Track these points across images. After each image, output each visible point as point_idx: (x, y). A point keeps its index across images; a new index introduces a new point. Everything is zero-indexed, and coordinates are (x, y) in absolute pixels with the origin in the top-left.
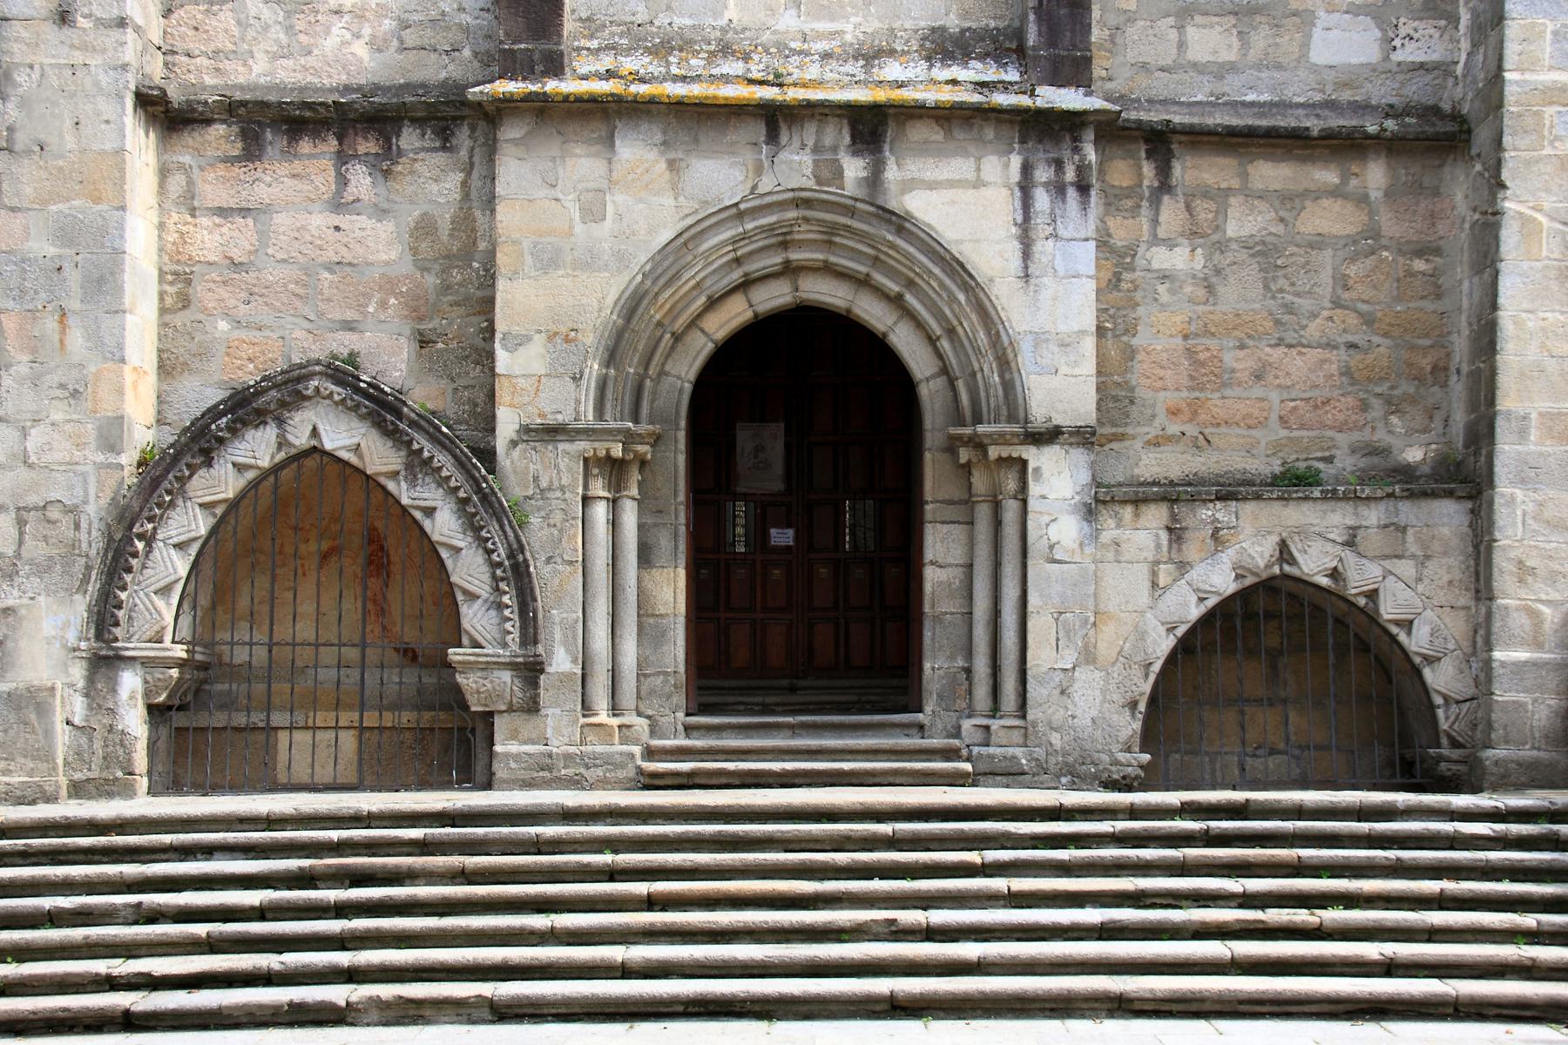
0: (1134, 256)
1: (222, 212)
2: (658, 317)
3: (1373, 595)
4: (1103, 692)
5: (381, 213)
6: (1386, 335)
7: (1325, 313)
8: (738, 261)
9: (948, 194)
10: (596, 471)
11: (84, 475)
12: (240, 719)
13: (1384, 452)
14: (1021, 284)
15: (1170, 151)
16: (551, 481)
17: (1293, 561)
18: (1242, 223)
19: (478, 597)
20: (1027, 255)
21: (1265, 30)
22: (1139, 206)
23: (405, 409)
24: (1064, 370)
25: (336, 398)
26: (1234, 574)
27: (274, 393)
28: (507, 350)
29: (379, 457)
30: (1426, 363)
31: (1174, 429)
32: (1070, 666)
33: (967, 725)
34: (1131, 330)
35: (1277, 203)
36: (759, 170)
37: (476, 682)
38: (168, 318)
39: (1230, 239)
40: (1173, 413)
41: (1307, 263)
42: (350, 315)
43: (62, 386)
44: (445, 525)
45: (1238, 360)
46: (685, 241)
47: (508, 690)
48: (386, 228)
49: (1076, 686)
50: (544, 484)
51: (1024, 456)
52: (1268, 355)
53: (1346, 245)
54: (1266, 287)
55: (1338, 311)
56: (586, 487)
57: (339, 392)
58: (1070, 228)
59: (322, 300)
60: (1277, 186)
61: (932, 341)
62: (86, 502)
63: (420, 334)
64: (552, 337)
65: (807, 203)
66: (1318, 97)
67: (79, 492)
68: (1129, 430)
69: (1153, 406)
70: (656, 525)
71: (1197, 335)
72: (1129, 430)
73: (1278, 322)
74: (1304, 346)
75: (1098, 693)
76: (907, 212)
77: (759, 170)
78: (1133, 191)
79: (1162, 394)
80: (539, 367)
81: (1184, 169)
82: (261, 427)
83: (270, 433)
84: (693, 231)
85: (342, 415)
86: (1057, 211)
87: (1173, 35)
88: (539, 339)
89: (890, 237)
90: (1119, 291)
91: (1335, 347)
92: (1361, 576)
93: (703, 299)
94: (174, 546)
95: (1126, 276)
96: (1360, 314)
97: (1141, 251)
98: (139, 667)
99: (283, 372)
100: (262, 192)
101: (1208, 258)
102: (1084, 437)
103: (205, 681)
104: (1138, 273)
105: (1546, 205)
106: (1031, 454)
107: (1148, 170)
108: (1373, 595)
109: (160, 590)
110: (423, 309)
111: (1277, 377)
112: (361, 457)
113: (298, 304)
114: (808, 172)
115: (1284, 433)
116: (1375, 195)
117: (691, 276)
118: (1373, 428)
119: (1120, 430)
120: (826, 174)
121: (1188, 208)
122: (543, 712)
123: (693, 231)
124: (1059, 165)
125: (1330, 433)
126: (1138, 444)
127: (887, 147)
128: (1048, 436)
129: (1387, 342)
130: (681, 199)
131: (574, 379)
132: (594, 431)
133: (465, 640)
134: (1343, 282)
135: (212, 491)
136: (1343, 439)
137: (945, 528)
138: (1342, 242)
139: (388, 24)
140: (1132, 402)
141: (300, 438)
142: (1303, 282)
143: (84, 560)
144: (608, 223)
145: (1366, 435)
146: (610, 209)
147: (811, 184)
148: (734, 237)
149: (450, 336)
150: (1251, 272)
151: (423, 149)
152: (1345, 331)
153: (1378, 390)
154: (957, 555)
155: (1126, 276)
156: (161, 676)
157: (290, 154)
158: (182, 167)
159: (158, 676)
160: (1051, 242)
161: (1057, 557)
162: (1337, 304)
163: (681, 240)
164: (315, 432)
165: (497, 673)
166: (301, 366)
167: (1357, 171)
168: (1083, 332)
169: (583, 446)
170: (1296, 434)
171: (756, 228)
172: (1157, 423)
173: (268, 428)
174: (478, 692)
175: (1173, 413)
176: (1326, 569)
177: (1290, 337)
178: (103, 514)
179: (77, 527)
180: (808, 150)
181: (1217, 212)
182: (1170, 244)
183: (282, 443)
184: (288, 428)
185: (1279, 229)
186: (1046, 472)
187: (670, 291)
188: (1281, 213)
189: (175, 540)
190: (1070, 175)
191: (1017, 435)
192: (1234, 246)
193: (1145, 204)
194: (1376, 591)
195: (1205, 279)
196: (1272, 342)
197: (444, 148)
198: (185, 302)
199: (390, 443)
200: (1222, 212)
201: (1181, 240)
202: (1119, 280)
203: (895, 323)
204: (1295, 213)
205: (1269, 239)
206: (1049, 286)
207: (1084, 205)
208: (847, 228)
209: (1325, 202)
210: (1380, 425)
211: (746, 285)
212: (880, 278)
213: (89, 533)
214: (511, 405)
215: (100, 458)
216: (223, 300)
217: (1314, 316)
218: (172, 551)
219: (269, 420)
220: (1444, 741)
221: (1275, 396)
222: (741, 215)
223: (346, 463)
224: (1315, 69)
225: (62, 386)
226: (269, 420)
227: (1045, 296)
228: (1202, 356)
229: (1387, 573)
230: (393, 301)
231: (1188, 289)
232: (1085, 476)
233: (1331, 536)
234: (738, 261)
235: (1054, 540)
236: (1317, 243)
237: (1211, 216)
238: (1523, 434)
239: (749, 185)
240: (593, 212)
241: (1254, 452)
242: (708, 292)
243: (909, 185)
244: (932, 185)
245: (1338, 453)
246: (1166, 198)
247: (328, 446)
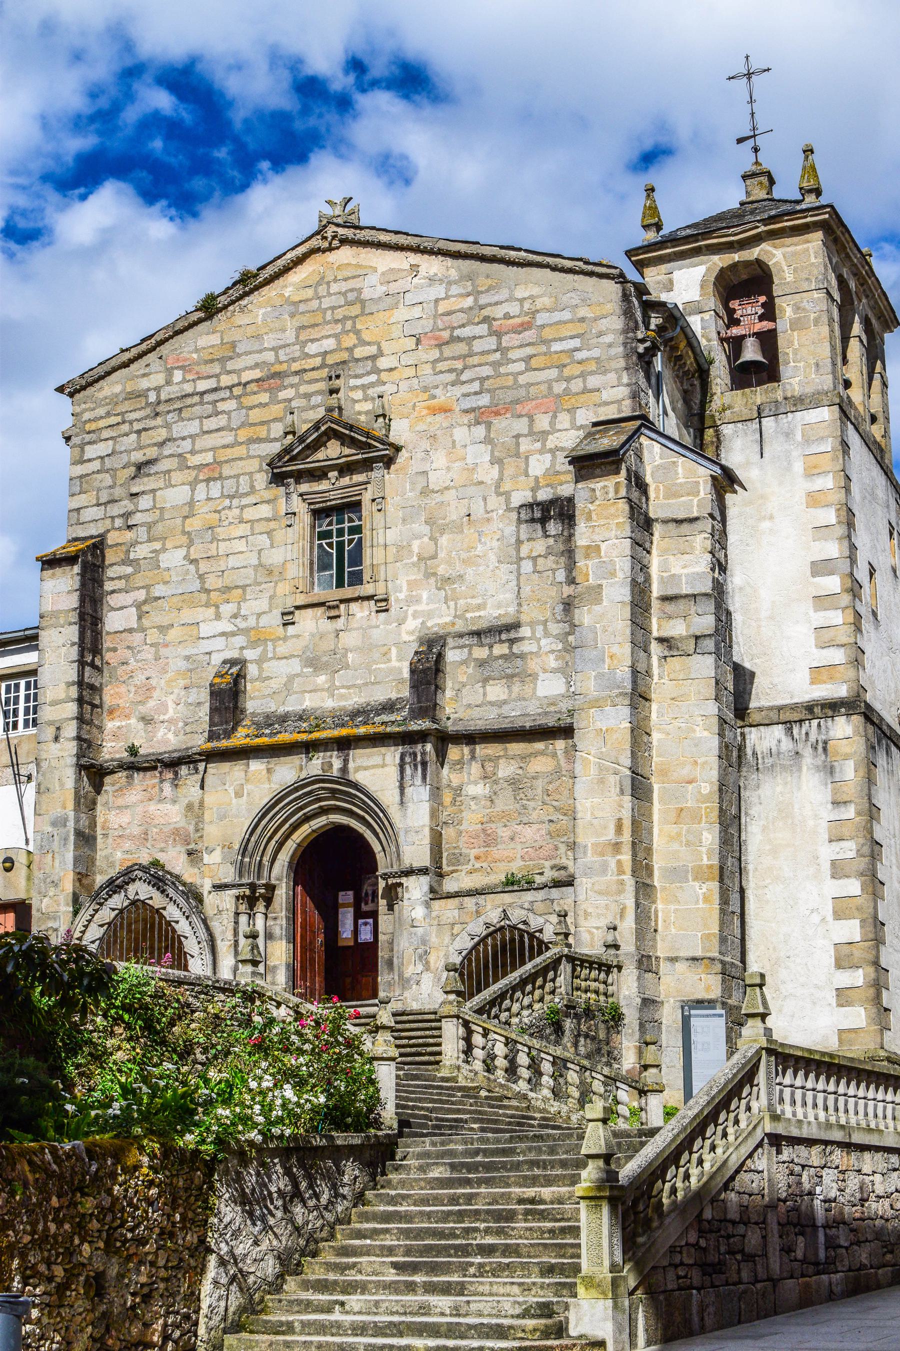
3: (541, 931)
5: (174, 802)
9: (372, 771)
17: (509, 919)
18: (506, 770)
21: (518, 684)
24: (417, 842)
29: (158, 900)
31: (478, 865)
34: (460, 823)
36: (301, 769)
40: (477, 858)
42: (163, 845)
44: (183, 927)
56: (237, 908)
66: (540, 711)
72: (459, 868)
77: (301, 769)
80: (219, 860)
87: (481, 690)
88: (219, 849)
101: (491, 788)
105: (593, 752)
106: (404, 880)
108: (541, 931)
120: (326, 768)
121: (483, 766)
126: (463, 873)
128: (409, 873)
129: (565, 818)
136: (548, 864)
139: (181, 724)
142: (530, 794)
144: (245, 797)
147: (320, 772)
150: (509, 792)
155: (458, 799)
162: (544, 803)
164: (137, 894)
169: (235, 892)
175: (477, 858)
177: (525, 820)
182: (476, 783)
185: (520, 772)
200: (496, 766)
210: (563, 856)
211: (307, 819)
217: (534, 809)
221: (519, 847)
222: (296, 790)
224: (539, 699)
227: (409, 811)
232: (426, 888)
238: (585, 853)
243: (357, 770)
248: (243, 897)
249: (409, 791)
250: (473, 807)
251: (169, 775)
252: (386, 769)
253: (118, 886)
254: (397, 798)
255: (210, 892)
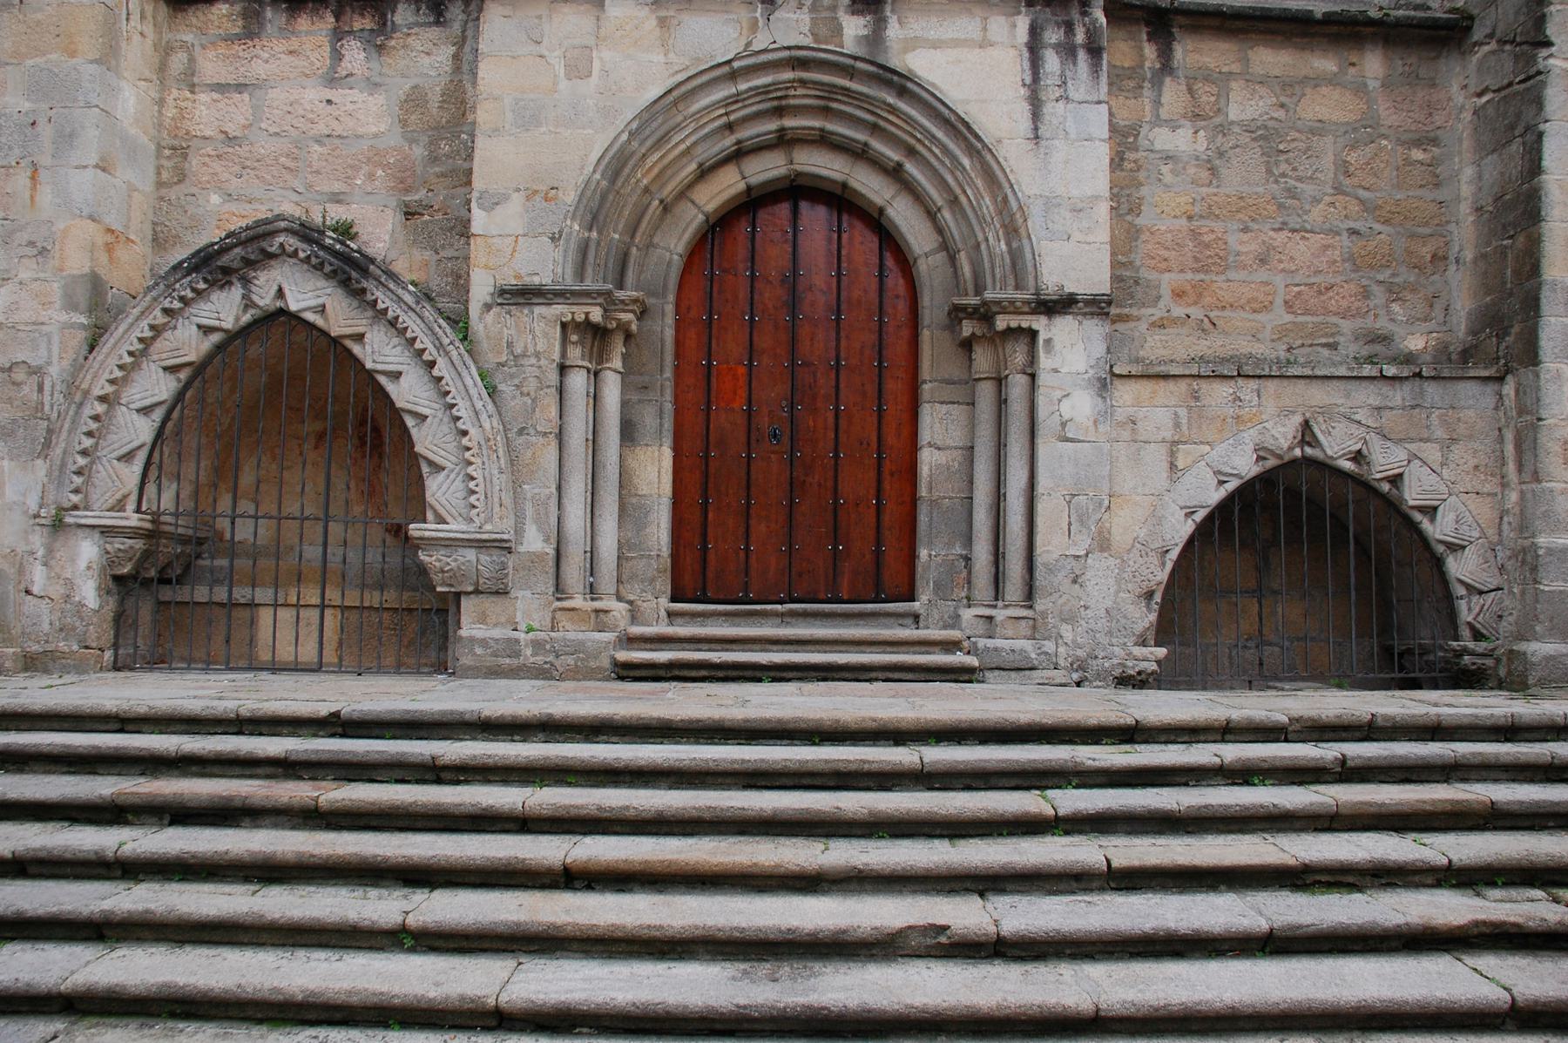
0: (1136, 136)
1: (221, 88)
2: (645, 182)
3: (1396, 480)
4: (1118, 580)
5: (373, 86)
6: (1386, 222)
7: (1327, 199)
8: (730, 127)
10: (574, 338)
11: (49, 336)
12: (221, 594)
13: (1385, 339)
14: (1031, 145)
15: (1171, 34)
16: (526, 347)
17: (1314, 442)
18: (1244, 106)
19: (444, 469)
20: (1036, 115)
22: (1142, 87)
23: (372, 267)
24: (1077, 236)
25: (302, 255)
26: (1255, 456)
27: (237, 250)
28: (484, 210)
30: (1426, 251)
31: (1179, 311)
32: (1082, 553)
33: (967, 614)
35: (1278, 89)
36: (754, 26)
37: (440, 561)
38: (163, 191)
39: (1232, 123)
40: (1179, 294)
41: (1308, 149)
42: (337, 187)
43: (32, 244)
45: (1242, 243)
46: (675, 98)
47: (474, 570)
48: (377, 102)
49: (1089, 575)
50: (518, 351)
51: (1035, 326)
52: (1272, 239)
53: (1346, 132)
54: (1269, 171)
55: (1340, 197)
56: (564, 354)
57: (304, 250)
58: (1082, 90)
59: (311, 172)
60: (1276, 72)
61: (932, 215)
62: (49, 363)
63: (406, 206)
64: (531, 195)
65: (803, 64)
67: (43, 352)
68: (1134, 312)
69: (1159, 286)
70: (640, 401)
71: (1201, 217)
72: (1134, 312)
73: (1281, 206)
74: (1307, 231)
75: (1112, 581)
76: (910, 71)
78: (1134, 72)
79: (1167, 275)
80: (517, 226)
81: (1185, 51)
82: (227, 287)
83: (237, 292)
84: (683, 89)
85: (309, 274)
86: (1068, 73)
88: (517, 200)
89: (891, 100)
90: (1122, 170)
91: (1338, 234)
92: (1384, 460)
93: (694, 166)
94: (138, 411)
95: (1130, 155)
96: (1362, 202)
97: (1143, 131)
98: (97, 535)
99: (248, 228)
100: (259, 69)
101: (1211, 140)
102: (1098, 307)
103: (198, 556)
104: (1141, 154)
106: (1039, 323)
107: (1150, 51)
108: (1396, 480)
109: (124, 456)
110: (410, 181)
111: (1280, 261)
112: (326, 320)
113: (288, 177)
114: (806, 30)
115: (1289, 318)
116: (1373, 84)
117: (681, 140)
118: (1376, 316)
119: (1126, 311)
120: (823, 31)
121: (1190, 90)
122: (513, 594)
123: (683, 89)
124: (1069, 27)
125: (1334, 319)
126: (1143, 326)
127: (888, 8)
130: (671, 55)
131: (553, 239)
132: (574, 293)
133: (430, 515)
134: (1344, 168)
135: (176, 353)
137: (945, 408)
138: (1342, 130)
140: (1137, 283)
141: (265, 299)
143: (46, 423)
144: (594, 79)
145: (1369, 322)
146: (596, 65)
147: (808, 41)
148: (727, 98)
149: (436, 207)
150: (1254, 156)
151: (417, 24)
152: (1346, 216)
153: (1380, 277)
154: (956, 437)
155: (1130, 155)
156: (122, 547)
157: (287, 32)
158: (184, 45)
159: (117, 546)
160: (1061, 104)
161: (1070, 435)
162: (1339, 190)
163: (670, 98)
164: (280, 293)
165: (461, 551)
166: (266, 222)
167: (1354, 60)
168: (1097, 197)
170: (1300, 319)
171: (751, 89)
172: (1161, 304)
173: (233, 288)
174: (443, 571)
175: (1179, 294)
176: (1350, 452)
177: (1294, 222)
178: (65, 375)
179: (41, 389)
180: (805, 9)
181: (1218, 95)
183: (248, 303)
184: (254, 289)
185: (1280, 114)
186: (1057, 345)
187: (656, 156)
188: (1283, 99)
189: (138, 405)
190: (1080, 37)
191: (1028, 303)
192: (1237, 129)
193: (1146, 84)
194: (1400, 475)
195: (1209, 161)
196: (1277, 226)
197: (437, 23)
198: (181, 177)
199: (355, 303)
200: (1223, 94)
201: (1183, 122)
202: (1122, 159)
203: (893, 197)
204: (1295, 99)
205: (1271, 124)
206: (1060, 150)
207: (1095, 68)
208: (846, 91)
209: (1324, 90)
210: (1382, 312)
211: (739, 154)
212: (878, 146)
213: (52, 395)
214: (486, 267)
215: (64, 317)
216: (216, 174)
217: (1316, 201)
218: (135, 415)
219: (235, 280)
220: (1465, 632)
221: (1279, 281)
222: (733, 76)
223: (312, 326)
225: (32, 244)
226: (235, 280)
228: (1206, 238)
229: (1411, 457)
230: (380, 172)
231: (1191, 171)
232: (1099, 349)
233: (1357, 417)
234: (730, 127)
235: (1066, 417)
236: (1319, 129)
237: (1213, 99)
239: (743, 42)
240: (578, 69)
241: (1260, 336)
242: (699, 159)
243: (912, 44)
244: (936, 45)
245: (1341, 339)
246: (1168, 80)
247: (293, 307)
248: (588, 327)
249: (1054, 110)
250: (1168, 178)
251: (363, 23)
252: (995, 53)
253: (226, 271)
254: (1025, 124)
255: (488, 307)
